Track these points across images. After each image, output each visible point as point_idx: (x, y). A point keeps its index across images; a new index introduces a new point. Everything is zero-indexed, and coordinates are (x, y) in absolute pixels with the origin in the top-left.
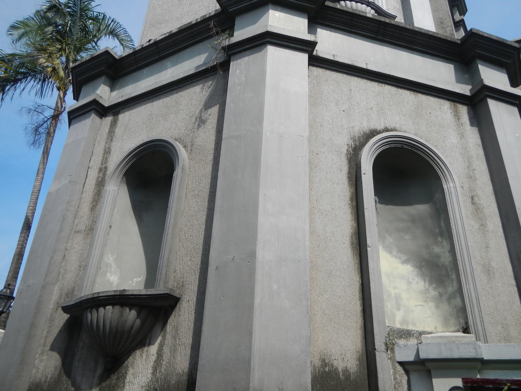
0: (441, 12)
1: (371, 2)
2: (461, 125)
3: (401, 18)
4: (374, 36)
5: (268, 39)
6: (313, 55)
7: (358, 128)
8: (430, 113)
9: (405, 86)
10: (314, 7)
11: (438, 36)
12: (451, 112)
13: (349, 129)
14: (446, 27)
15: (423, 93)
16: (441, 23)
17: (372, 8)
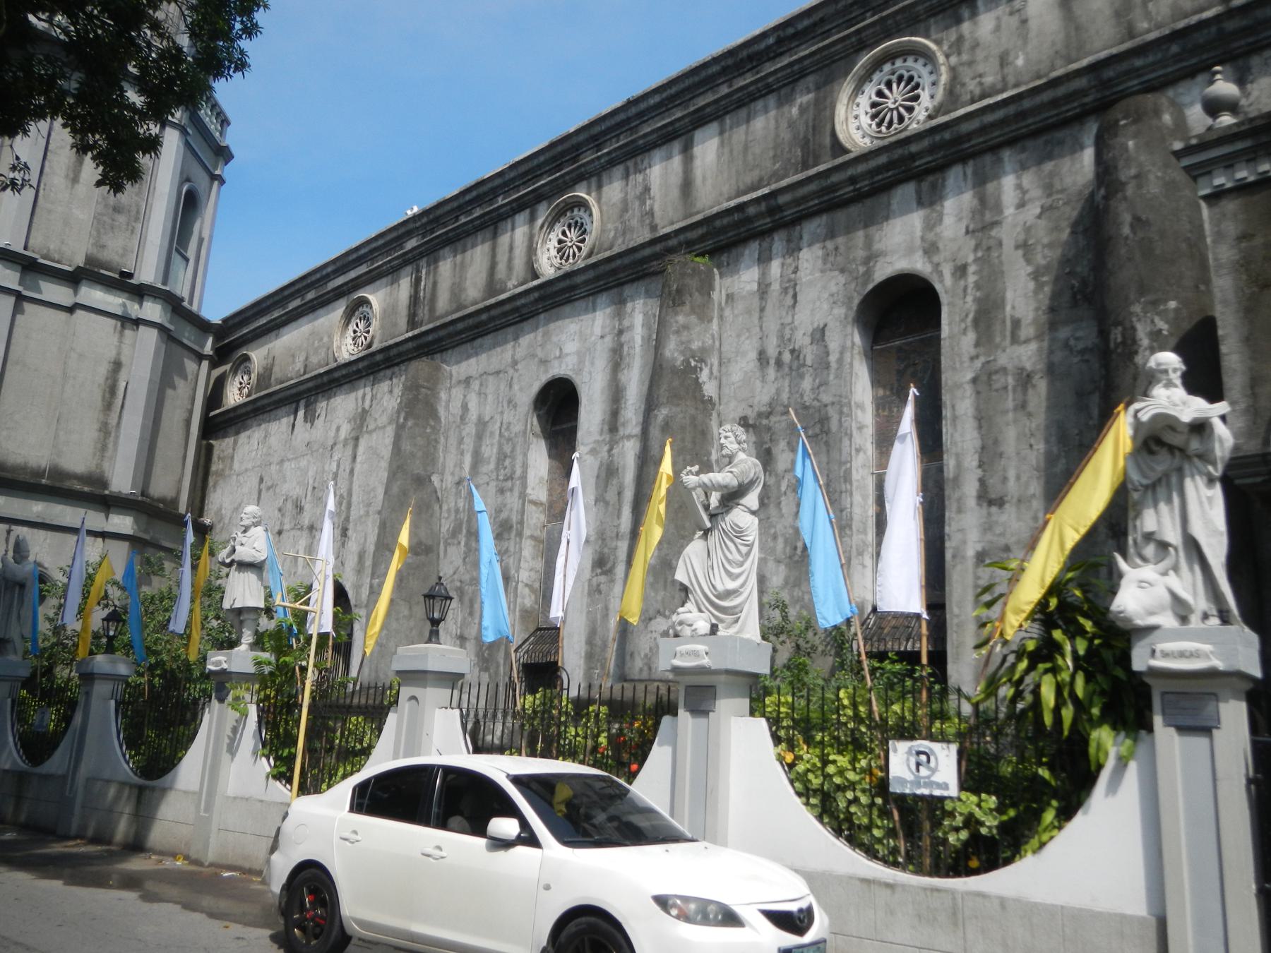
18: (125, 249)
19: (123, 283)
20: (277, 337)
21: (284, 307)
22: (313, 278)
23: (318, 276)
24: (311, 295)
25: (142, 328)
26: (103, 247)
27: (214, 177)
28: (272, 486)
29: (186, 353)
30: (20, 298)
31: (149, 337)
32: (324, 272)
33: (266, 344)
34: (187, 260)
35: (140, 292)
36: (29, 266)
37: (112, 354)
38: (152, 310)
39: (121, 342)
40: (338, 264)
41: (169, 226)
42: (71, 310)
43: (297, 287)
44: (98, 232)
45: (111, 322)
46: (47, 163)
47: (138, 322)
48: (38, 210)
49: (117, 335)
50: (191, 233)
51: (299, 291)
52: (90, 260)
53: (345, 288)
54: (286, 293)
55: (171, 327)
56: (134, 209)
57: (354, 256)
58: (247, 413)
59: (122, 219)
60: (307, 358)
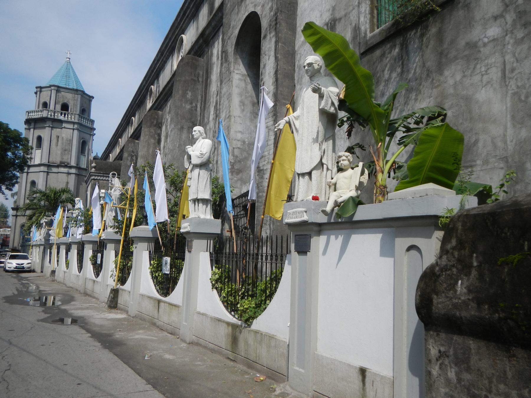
18: (68, 158)
19: (67, 166)
25: (71, 175)
26: (63, 159)
27: (91, 135)
29: (84, 177)
30: (48, 173)
31: (73, 176)
34: (85, 156)
35: (71, 167)
36: (49, 166)
37: (67, 181)
38: (73, 171)
39: (68, 178)
41: (77, 151)
42: (58, 173)
44: (62, 156)
45: (65, 174)
46: (51, 143)
47: (71, 173)
48: (50, 153)
50: (85, 149)
52: (61, 162)
55: (78, 173)
56: (69, 149)
59: (66, 152)
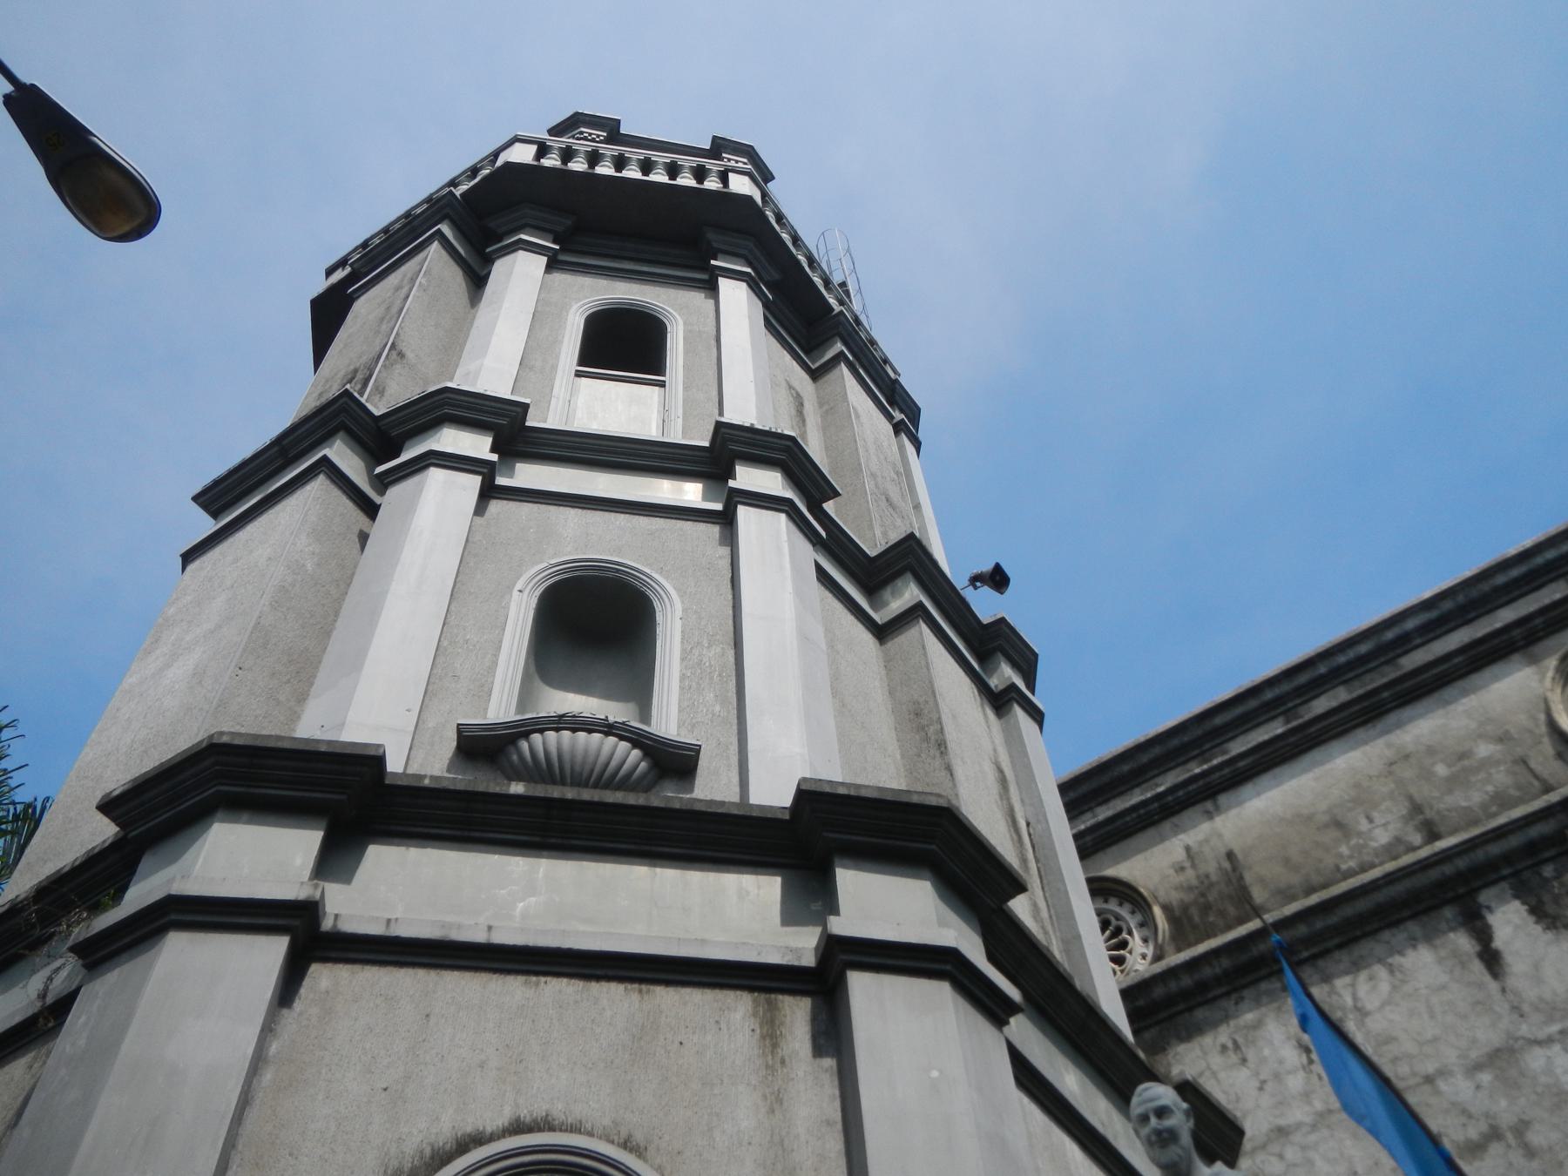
0: (915, 687)
1: (616, 722)
2: (778, 1065)
3: (731, 743)
4: (537, 839)
5: (173, 917)
6: (322, 932)
7: (419, 1139)
8: (681, 1043)
9: (610, 973)
10: (343, 797)
11: (719, 811)
12: (752, 1027)
13: (386, 1149)
14: (927, 726)
15: (668, 983)
16: (917, 714)
17: (622, 738)
20: (1209, 815)
21: (1203, 756)
22: (1342, 659)
23: (1363, 649)
24: (1321, 705)
28: (1494, 1134)
32: (1390, 635)
33: (1163, 839)
40: (1448, 605)
43: (1269, 695)
49: (980, 709)
51: (1278, 701)
53: (1516, 633)
54: (1219, 720)
57: (1515, 573)
58: (1202, 987)
60: (1416, 809)
